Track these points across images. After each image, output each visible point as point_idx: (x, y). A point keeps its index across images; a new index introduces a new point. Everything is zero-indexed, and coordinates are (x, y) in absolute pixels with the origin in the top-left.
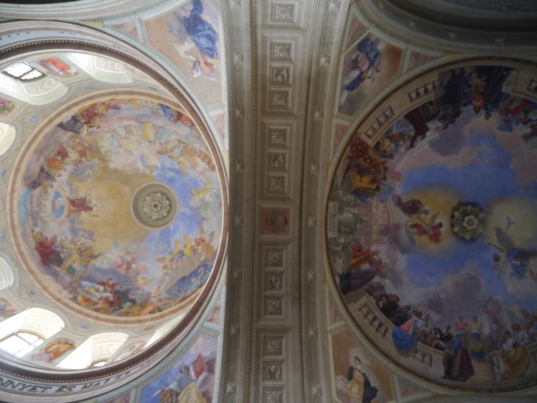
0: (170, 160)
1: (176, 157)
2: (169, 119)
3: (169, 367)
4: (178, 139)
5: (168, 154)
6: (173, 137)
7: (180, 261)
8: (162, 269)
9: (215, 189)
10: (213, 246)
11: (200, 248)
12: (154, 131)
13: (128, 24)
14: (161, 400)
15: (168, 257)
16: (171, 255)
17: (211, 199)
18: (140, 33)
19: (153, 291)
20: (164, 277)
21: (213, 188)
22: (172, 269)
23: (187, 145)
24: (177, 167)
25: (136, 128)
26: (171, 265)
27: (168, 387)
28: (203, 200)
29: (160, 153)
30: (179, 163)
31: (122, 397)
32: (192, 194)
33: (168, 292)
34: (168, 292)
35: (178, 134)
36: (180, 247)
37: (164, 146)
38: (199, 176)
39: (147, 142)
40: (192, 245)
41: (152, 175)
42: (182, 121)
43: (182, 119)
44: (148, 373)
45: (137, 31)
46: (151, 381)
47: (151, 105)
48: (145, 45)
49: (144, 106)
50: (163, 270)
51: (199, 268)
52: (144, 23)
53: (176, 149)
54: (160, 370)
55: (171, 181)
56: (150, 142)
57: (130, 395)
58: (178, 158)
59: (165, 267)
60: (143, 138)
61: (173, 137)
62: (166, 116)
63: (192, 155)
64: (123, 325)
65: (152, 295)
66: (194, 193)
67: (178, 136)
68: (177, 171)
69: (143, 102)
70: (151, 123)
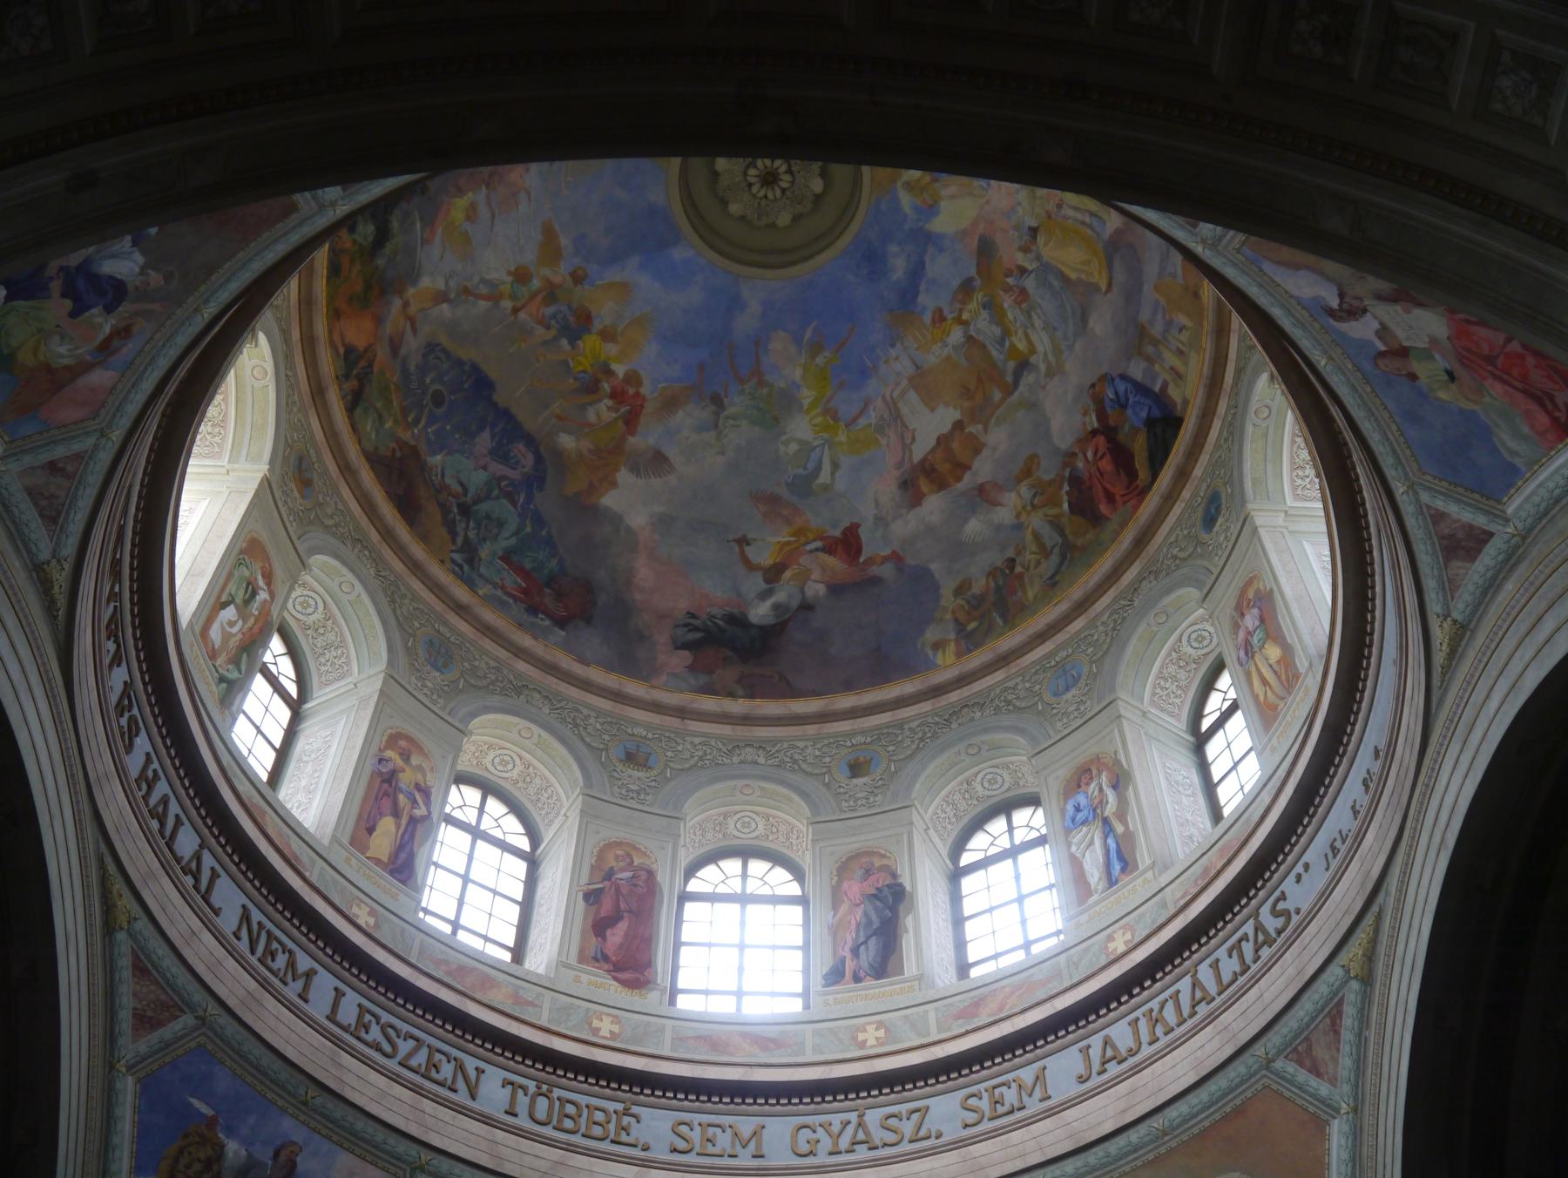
0: (956, 283)
1: (965, 316)
2: (1105, 378)
3: (280, 1102)
4: (1033, 360)
5: (978, 282)
6: (1042, 342)
7: (553, 332)
8: (513, 269)
9: (833, 474)
10: (614, 484)
11: (602, 411)
12: (1073, 276)
13: (1335, 1060)
14: (186, 1136)
15: (560, 274)
16: (569, 281)
17: (793, 447)
18: (1302, 1076)
19: (425, 282)
20: (484, 290)
21: (835, 466)
22: (516, 311)
23: (1009, 390)
24: (926, 301)
25: (1092, 214)
26: (533, 296)
27: (227, 1137)
28: (787, 401)
29: (986, 250)
30: (939, 317)
31: (163, 997)
32: (816, 348)
33: (431, 348)
34: (431, 348)
35: (1050, 374)
36: (605, 312)
37: (1010, 280)
38: (883, 397)
39: (1034, 224)
40: (615, 367)
41: (899, 184)
42: (1094, 433)
43: (1101, 439)
44: (249, 1036)
45: (1310, 1071)
46: (229, 1062)
47: (1170, 359)
48: (1267, 1068)
49: (1169, 324)
50: (509, 273)
51: (530, 441)
52: (1325, 1117)
53: (997, 331)
54: (265, 1075)
55: (872, 260)
56: (1034, 231)
57: (178, 1017)
58: (959, 321)
59: (521, 276)
60: (1049, 217)
61: (1042, 342)
62: (1123, 377)
63: (967, 393)
64: (296, 335)
65: (411, 291)
66: (820, 360)
67: (1043, 367)
68: (908, 295)
69: (1184, 336)
70: (1104, 288)
